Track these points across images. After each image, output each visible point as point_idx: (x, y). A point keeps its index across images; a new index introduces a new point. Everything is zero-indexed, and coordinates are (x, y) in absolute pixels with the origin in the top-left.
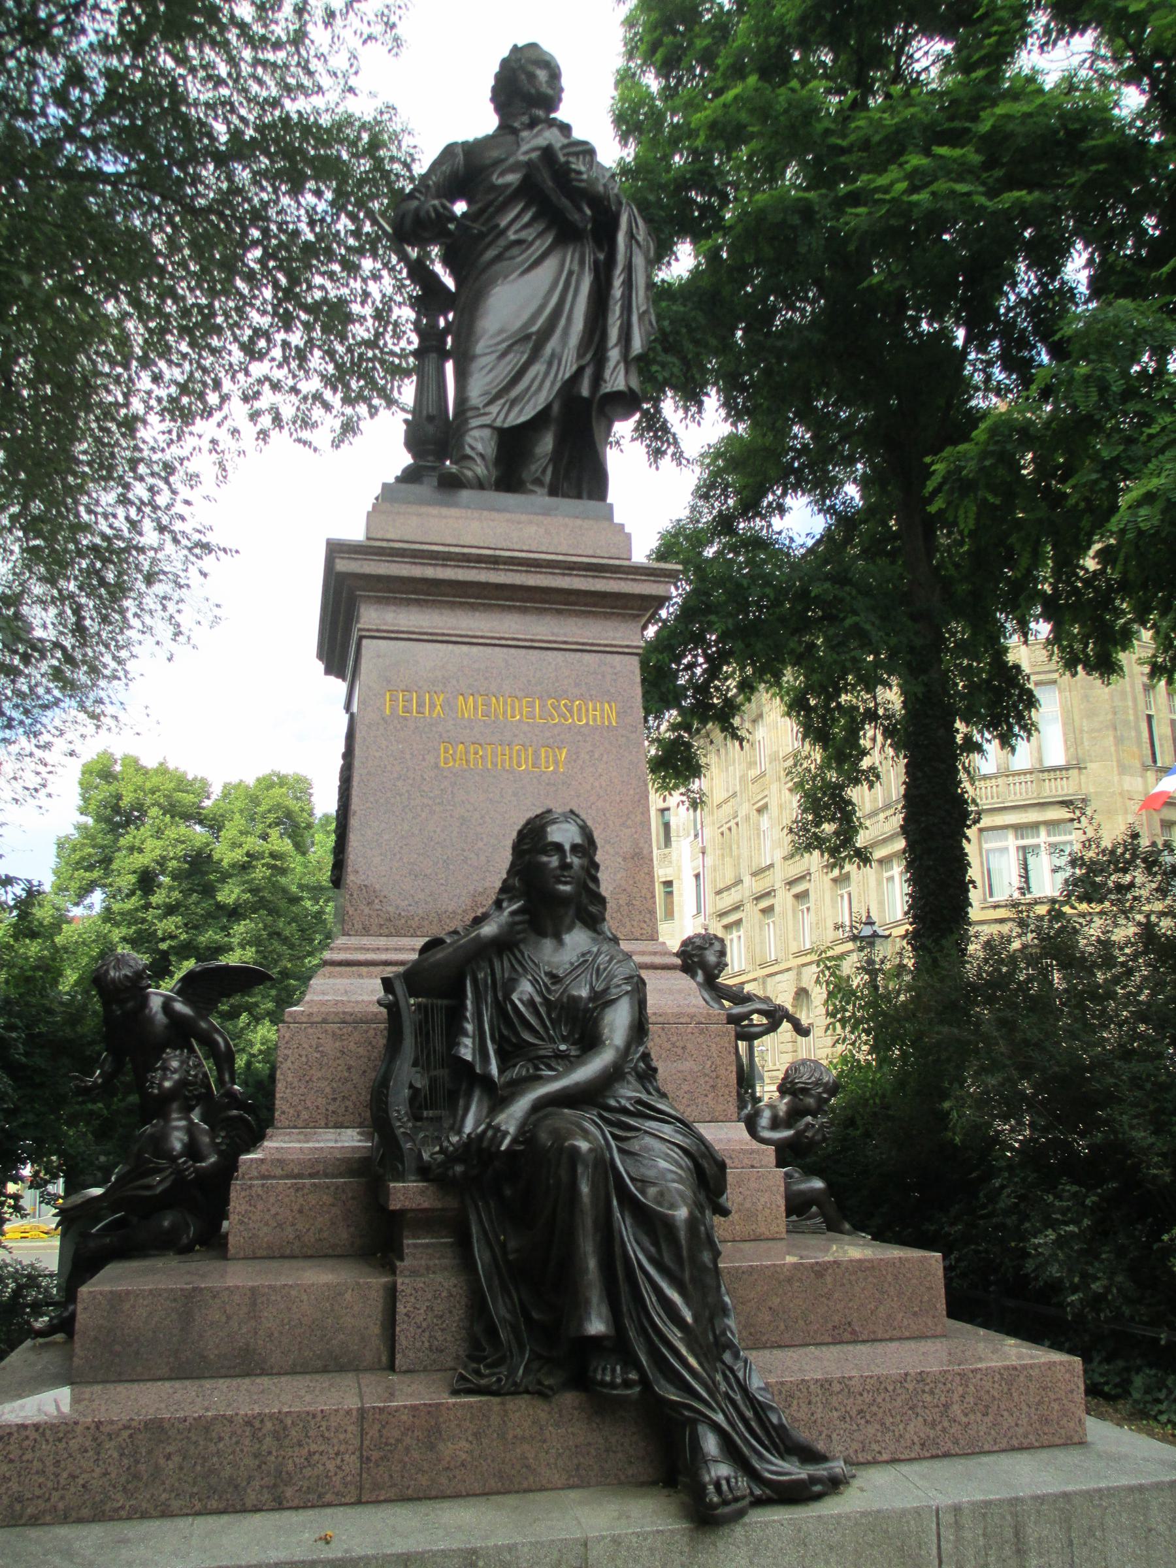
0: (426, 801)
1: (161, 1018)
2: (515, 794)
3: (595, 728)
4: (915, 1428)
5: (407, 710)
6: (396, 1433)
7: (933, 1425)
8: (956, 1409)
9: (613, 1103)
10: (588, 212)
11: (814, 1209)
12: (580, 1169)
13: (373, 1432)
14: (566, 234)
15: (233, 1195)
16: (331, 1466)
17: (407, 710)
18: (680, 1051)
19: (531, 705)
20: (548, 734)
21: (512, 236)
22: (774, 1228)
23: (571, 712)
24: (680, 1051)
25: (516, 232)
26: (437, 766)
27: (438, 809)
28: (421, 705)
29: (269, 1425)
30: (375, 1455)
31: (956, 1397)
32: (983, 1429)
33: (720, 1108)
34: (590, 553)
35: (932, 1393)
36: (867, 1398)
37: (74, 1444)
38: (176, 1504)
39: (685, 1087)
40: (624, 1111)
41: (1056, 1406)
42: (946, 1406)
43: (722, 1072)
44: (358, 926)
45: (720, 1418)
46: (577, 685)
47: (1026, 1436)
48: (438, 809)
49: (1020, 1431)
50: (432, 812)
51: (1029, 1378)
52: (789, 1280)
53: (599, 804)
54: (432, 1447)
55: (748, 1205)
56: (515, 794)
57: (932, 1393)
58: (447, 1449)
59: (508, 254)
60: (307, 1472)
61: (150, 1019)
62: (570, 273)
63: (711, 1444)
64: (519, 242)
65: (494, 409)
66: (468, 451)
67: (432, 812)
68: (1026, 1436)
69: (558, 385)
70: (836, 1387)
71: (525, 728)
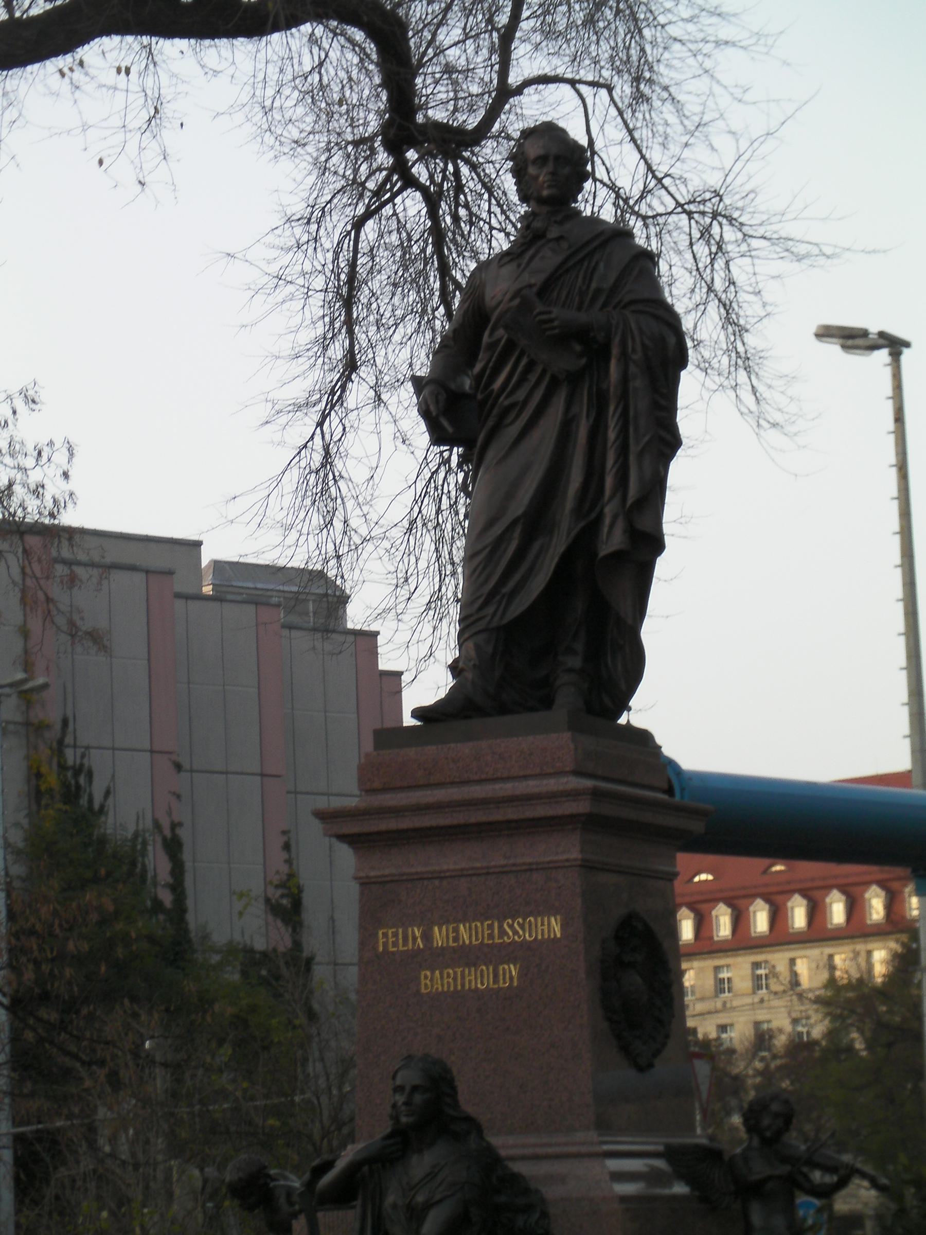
3: (543, 941)
10: (578, 348)
17: (395, 944)
19: (491, 927)
21: (504, 401)
25: (507, 397)
26: (418, 992)
64: (512, 406)
65: (490, 610)
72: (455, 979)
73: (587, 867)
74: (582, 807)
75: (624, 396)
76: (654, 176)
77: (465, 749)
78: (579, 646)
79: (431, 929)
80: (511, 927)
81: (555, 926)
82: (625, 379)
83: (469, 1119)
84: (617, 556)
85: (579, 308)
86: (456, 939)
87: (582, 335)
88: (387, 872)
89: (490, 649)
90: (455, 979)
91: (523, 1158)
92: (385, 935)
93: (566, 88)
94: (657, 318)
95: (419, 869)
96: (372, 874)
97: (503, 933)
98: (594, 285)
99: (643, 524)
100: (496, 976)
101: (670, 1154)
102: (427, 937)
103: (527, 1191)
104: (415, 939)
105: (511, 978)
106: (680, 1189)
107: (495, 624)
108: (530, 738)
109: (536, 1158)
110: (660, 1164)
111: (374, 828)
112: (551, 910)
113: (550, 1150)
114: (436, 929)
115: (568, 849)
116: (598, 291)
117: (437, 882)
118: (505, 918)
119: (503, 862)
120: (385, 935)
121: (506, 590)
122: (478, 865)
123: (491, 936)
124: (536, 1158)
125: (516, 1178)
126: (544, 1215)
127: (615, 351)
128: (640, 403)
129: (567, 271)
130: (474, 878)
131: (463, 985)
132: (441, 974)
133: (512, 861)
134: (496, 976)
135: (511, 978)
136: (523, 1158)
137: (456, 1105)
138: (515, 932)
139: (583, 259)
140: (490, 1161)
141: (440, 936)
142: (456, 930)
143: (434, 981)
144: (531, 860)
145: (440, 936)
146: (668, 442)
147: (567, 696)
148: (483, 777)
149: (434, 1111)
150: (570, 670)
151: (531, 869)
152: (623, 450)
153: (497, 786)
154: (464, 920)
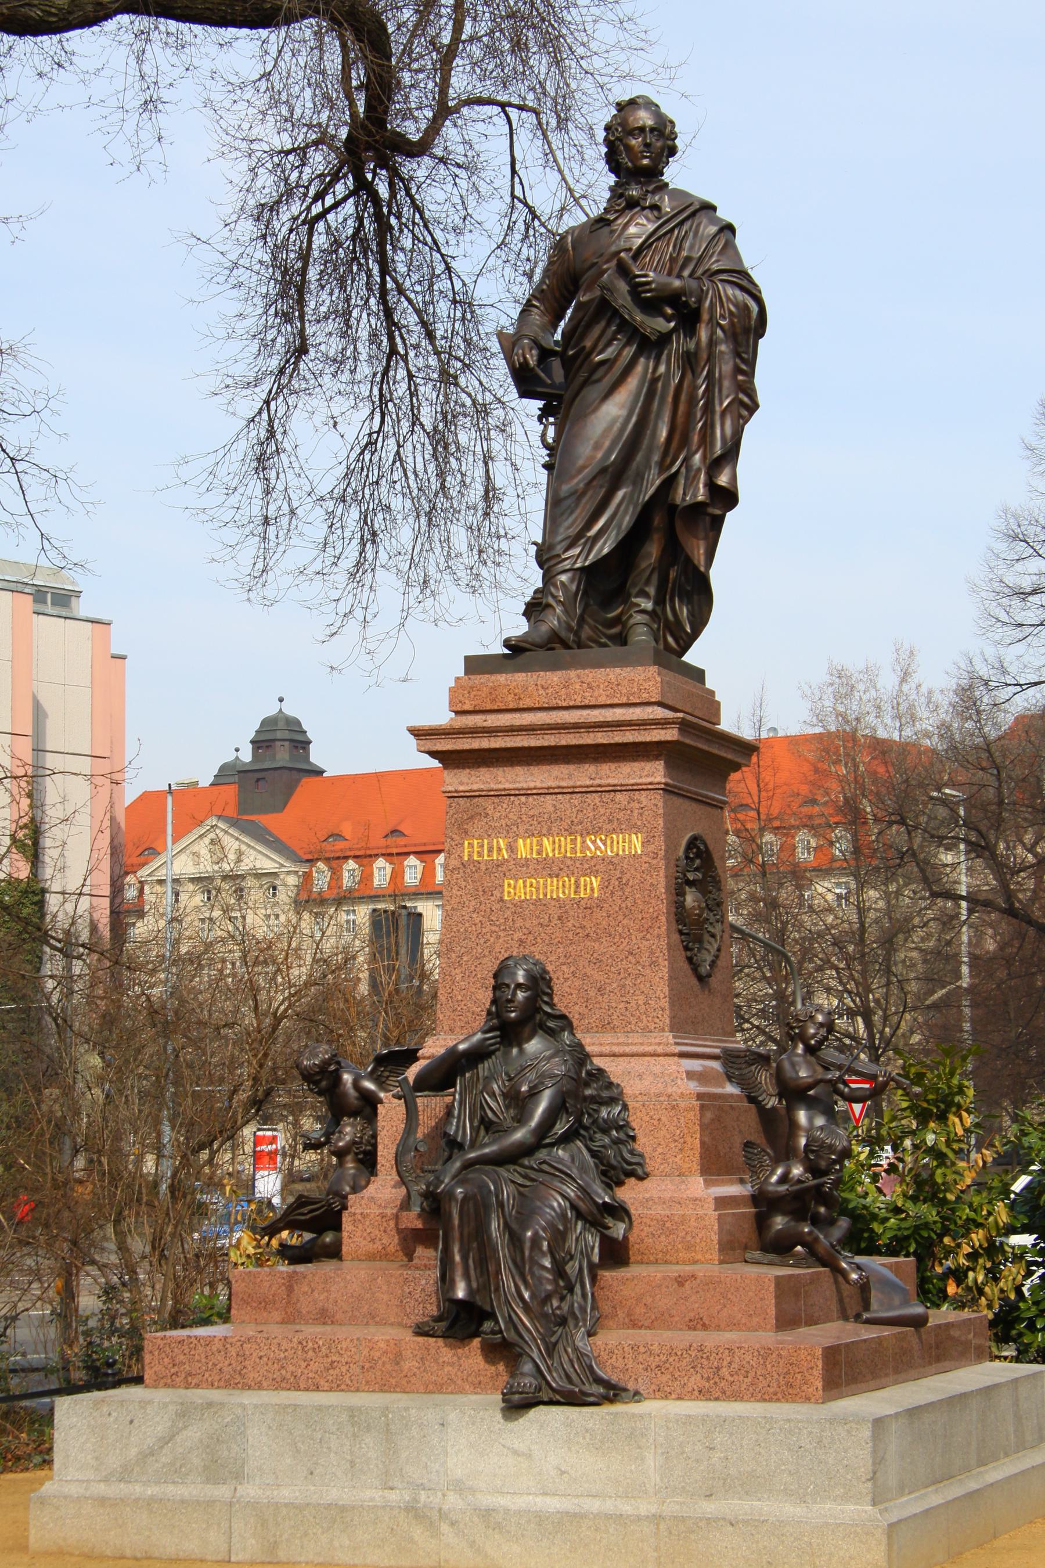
0: (494, 928)
1: (352, 1092)
2: (560, 918)
4: (695, 1381)
6: (378, 1354)
7: (708, 1379)
8: (724, 1372)
9: (526, 1162)
10: (669, 311)
11: (799, 1248)
12: (453, 1204)
13: (365, 1352)
15: (344, 1219)
16: (344, 1369)
17: (480, 854)
18: (656, 1123)
20: (586, 866)
22: (708, 1256)
23: (605, 844)
24: (656, 1123)
26: (502, 900)
27: (502, 934)
28: (490, 850)
29: (310, 1345)
30: (367, 1365)
31: (725, 1363)
32: (744, 1386)
33: (686, 1166)
34: (624, 700)
35: (708, 1358)
36: (664, 1358)
37: (214, 1349)
38: (265, 1384)
39: (660, 1150)
40: (532, 1168)
41: (799, 1376)
42: (718, 1369)
43: (688, 1139)
44: (446, 1028)
45: (535, 1355)
46: (610, 821)
47: (775, 1394)
48: (502, 934)
49: (771, 1390)
50: (498, 937)
51: (780, 1356)
52: (660, 1286)
53: (625, 922)
54: (398, 1363)
55: (689, 1238)
56: (560, 918)
57: (708, 1358)
58: (406, 1365)
59: (596, 377)
60: (331, 1372)
61: (345, 1094)
64: (602, 363)
65: (576, 551)
66: (551, 601)
67: (498, 937)
68: (775, 1394)
69: (639, 508)
70: (642, 1350)
71: (569, 862)
72: (538, 889)
73: (668, 790)
74: (671, 734)
76: (572, 196)
77: (554, 677)
78: (652, 590)
79: (516, 841)
80: (594, 842)
81: (636, 843)
82: (712, 342)
83: (563, 1017)
84: (698, 507)
85: (669, 274)
86: (539, 853)
87: (674, 299)
88: (475, 787)
89: (574, 587)
90: (538, 889)
92: (471, 845)
93: (496, 109)
94: (742, 288)
95: (507, 786)
96: (461, 788)
97: (584, 847)
98: (684, 253)
99: (723, 480)
100: (577, 886)
102: (512, 849)
103: (610, 1085)
104: (499, 849)
105: (592, 890)
106: (731, 1089)
107: (578, 565)
108: (618, 670)
110: (716, 1065)
111: (466, 747)
113: (627, 1049)
114: (521, 841)
115: (655, 772)
116: (688, 259)
117: (523, 798)
118: (588, 833)
119: (588, 782)
120: (471, 845)
122: (564, 784)
123: (574, 850)
125: (600, 1074)
126: (625, 1107)
127: (705, 316)
128: (725, 367)
129: (659, 239)
130: (560, 797)
131: (545, 895)
132: (524, 882)
133: (598, 782)
134: (577, 886)
135: (592, 890)
137: (552, 1005)
138: (597, 848)
139: (672, 230)
140: (580, 1056)
142: (540, 844)
143: (517, 890)
144: (615, 782)
145: (523, 848)
146: (747, 404)
147: (641, 635)
148: (572, 703)
149: (524, 1010)
150: (643, 611)
151: (615, 790)
152: (708, 408)
153: (585, 712)
154: (549, 833)
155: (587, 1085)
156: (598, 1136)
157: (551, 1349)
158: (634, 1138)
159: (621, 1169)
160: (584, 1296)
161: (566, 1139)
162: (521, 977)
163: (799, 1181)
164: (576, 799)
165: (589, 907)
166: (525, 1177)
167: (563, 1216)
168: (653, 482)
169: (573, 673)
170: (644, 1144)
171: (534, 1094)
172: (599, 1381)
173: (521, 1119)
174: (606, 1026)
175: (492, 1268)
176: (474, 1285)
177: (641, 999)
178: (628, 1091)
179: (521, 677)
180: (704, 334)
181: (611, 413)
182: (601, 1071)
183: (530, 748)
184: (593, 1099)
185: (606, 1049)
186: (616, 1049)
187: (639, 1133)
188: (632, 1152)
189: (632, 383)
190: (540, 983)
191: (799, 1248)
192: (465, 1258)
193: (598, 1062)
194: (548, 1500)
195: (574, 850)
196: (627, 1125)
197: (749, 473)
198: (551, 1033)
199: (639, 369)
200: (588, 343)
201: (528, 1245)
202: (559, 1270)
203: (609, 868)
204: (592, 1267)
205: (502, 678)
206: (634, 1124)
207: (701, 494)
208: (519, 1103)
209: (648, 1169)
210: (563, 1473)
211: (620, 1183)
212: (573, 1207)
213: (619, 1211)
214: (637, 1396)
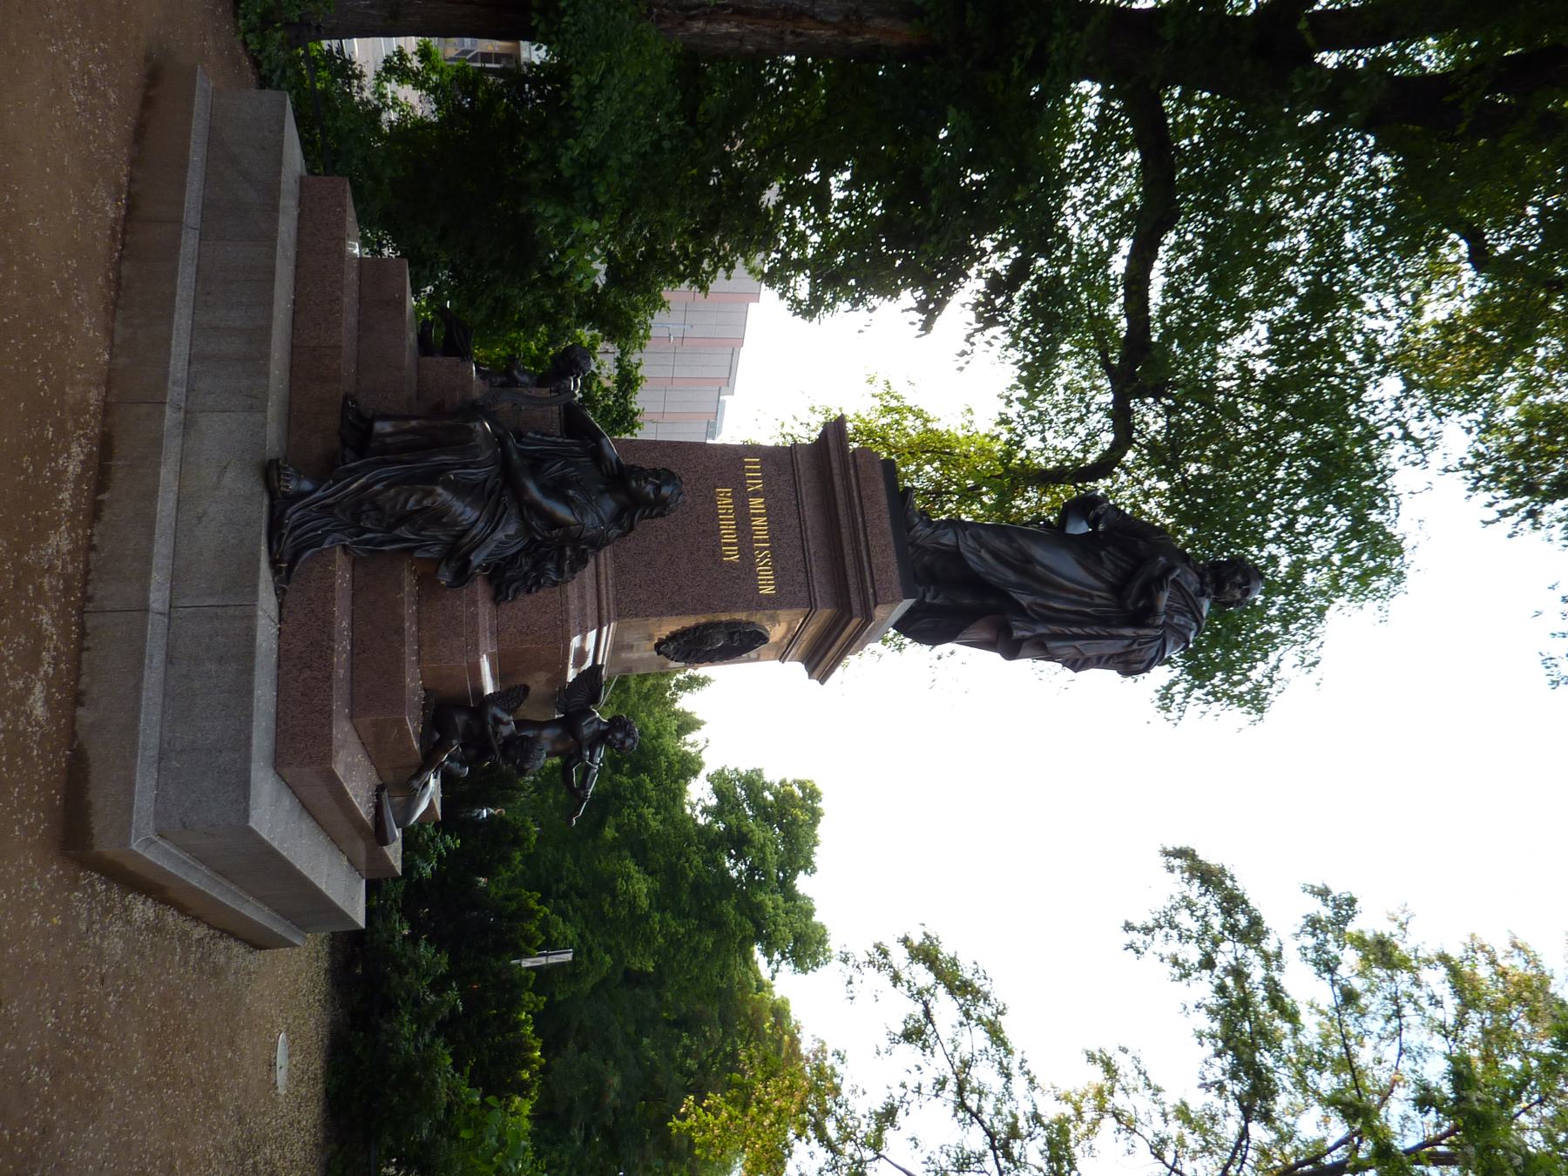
5: (750, 471)
10: (1141, 604)
11: (437, 736)
14: (1118, 590)
17: (750, 471)
19: (764, 541)
40: (501, 496)
42: (310, 667)
45: (319, 494)
62: (1091, 596)
63: (306, 485)
64: (1100, 558)
65: (970, 542)
75: (1111, 637)
81: (768, 590)
82: (1122, 637)
83: (632, 528)
86: (755, 515)
87: (1151, 610)
91: (597, 566)
97: (762, 549)
101: (596, 668)
102: (756, 494)
103: (573, 571)
106: (571, 675)
109: (597, 576)
110: (589, 663)
112: (778, 588)
113: (603, 586)
121: (983, 553)
123: (758, 541)
124: (597, 576)
126: (555, 584)
127: (1141, 632)
136: (597, 566)
137: (641, 518)
140: (597, 544)
141: (757, 503)
142: (760, 515)
145: (757, 503)
146: (1077, 664)
155: (574, 549)
156: (530, 561)
157: (326, 510)
158: (529, 592)
159: (504, 581)
160: (383, 543)
161: (527, 529)
162: (666, 491)
163: (496, 733)
164: (797, 542)
165: (715, 552)
166: (492, 492)
167: (456, 524)
168: (1025, 600)
169: (891, 538)
170: (525, 600)
171: (567, 502)
172: (296, 555)
173: (543, 489)
174: (620, 570)
175: (405, 457)
176: (389, 440)
177: (643, 597)
178: (569, 587)
179: (884, 500)
180: (1128, 632)
181: (1066, 565)
182: (586, 562)
183: (836, 505)
184: (562, 557)
185: (602, 569)
186: (603, 577)
187: (532, 597)
188: (517, 590)
189: (1091, 580)
190: (659, 507)
191: (437, 736)
192: (412, 431)
193: (592, 561)
194: (172, 504)
195: (758, 541)
196: (540, 586)
197: (1025, 667)
198: (616, 519)
199: (1098, 584)
200: (1110, 549)
201: (429, 487)
202: (405, 518)
203: (748, 565)
204: (410, 551)
205: (882, 486)
206: (541, 593)
207: (1017, 634)
208: (556, 489)
209: (503, 605)
210: (200, 518)
211: (490, 579)
212: (465, 532)
213: (462, 576)
214: (281, 593)
